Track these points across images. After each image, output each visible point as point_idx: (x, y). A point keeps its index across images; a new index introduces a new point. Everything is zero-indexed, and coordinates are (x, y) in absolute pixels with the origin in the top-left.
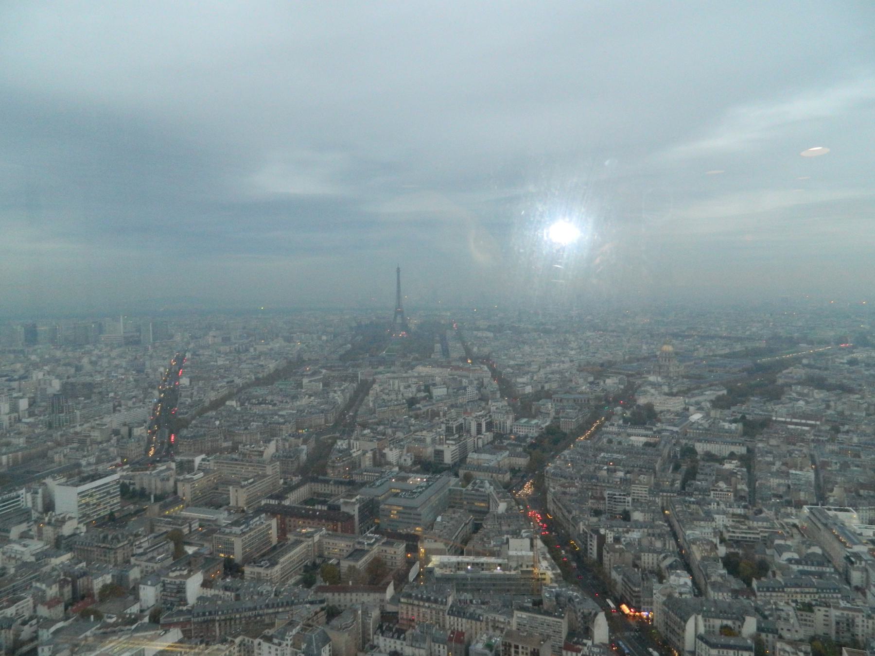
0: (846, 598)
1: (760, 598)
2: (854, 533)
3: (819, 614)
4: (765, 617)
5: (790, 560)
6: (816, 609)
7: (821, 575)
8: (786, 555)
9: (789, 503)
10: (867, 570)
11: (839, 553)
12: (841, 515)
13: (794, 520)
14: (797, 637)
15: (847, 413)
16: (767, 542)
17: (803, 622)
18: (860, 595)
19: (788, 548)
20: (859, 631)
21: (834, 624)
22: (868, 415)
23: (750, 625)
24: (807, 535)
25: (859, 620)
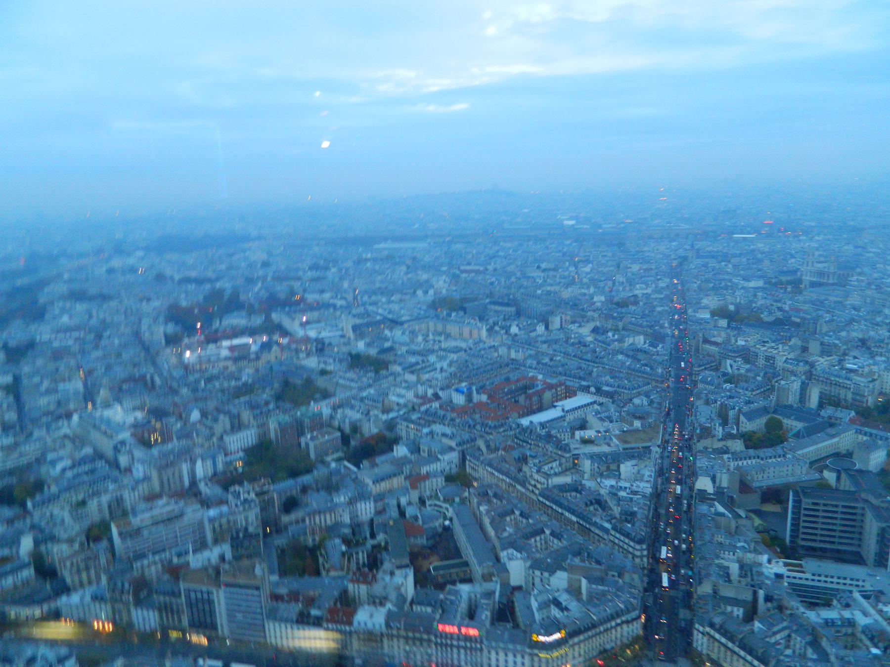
0: (115, 481)
1: (37, 516)
2: (119, 425)
3: (93, 505)
4: (42, 531)
5: (64, 470)
6: (90, 503)
7: (93, 471)
8: (59, 467)
9: (60, 417)
10: (130, 452)
11: (107, 446)
12: (108, 413)
13: (65, 430)
14: (74, 533)
15: (108, 320)
16: (40, 460)
17: (77, 518)
18: (128, 473)
19: (62, 459)
20: (128, 504)
21: (107, 509)
22: (126, 316)
23: (27, 544)
24: (78, 440)
25: (126, 495)
